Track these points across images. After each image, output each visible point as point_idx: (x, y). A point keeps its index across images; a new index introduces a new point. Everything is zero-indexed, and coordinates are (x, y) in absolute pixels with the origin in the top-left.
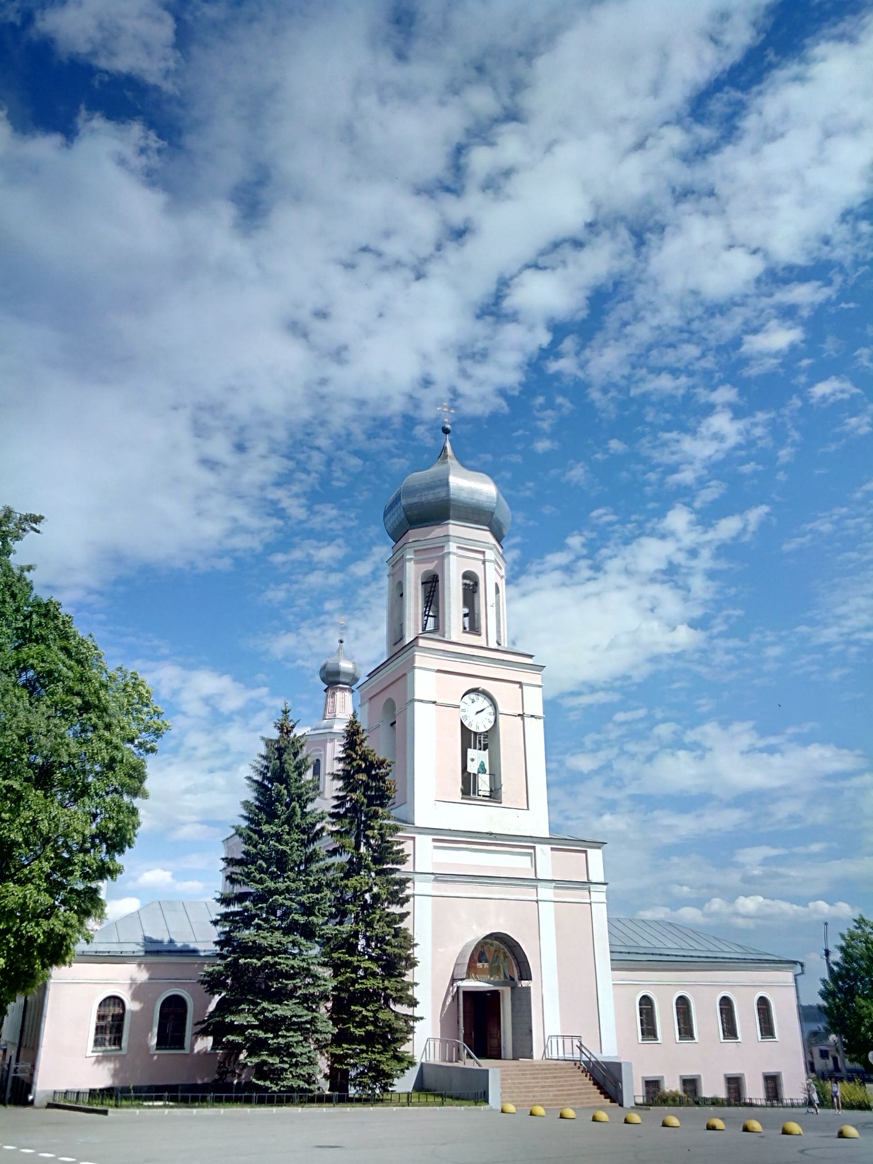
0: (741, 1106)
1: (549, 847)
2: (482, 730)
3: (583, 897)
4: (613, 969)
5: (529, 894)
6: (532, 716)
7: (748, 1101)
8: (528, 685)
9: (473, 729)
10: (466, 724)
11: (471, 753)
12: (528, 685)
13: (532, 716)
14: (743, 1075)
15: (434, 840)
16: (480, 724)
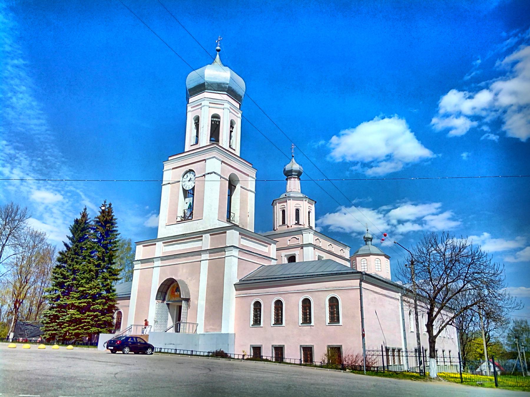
0: (261, 361)
1: (209, 234)
2: (191, 188)
3: (223, 255)
4: (236, 290)
5: (196, 258)
6: (208, 174)
7: (264, 358)
8: (208, 159)
9: (187, 189)
10: (184, 188)
11: (187, 199)
12: (208, 159)
13: (208, 174)
14: (313, 346)
15: (163, 243)
16: (189, 186)
